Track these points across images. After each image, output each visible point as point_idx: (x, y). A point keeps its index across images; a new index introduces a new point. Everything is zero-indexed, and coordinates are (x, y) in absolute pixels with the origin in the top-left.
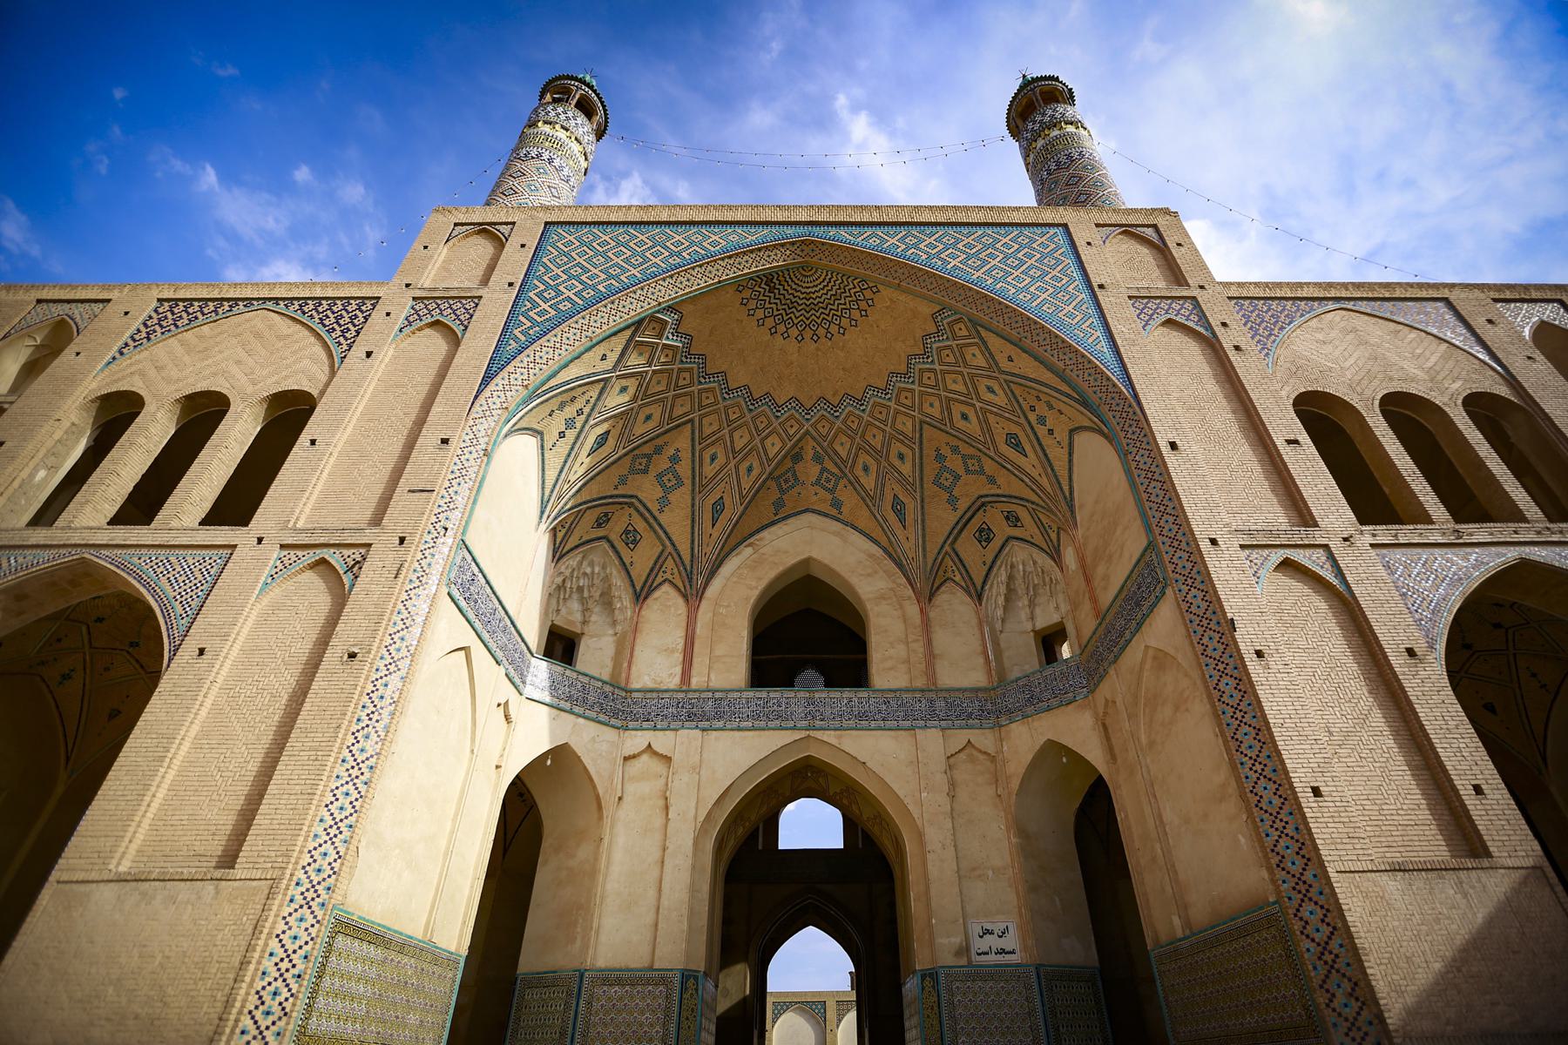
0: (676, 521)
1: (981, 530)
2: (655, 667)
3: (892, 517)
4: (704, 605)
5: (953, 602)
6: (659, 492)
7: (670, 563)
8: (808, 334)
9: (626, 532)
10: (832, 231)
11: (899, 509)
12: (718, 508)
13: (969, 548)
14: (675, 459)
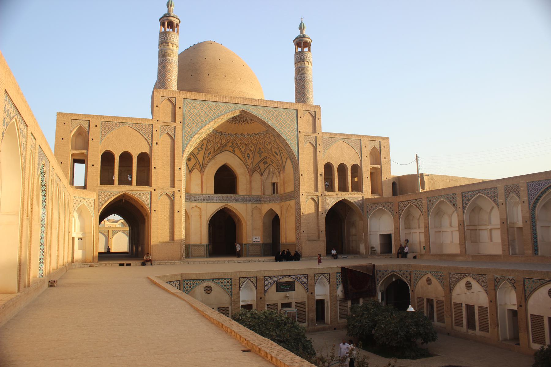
0: (200, 157)
2: (196, 189)
3: (246, 157)
4: (205, 174)
5: (257, 176)
10: (248, 106)
11: (248, 156)
12: (209, 154)
13: (262, 166)
14: (202, 145)
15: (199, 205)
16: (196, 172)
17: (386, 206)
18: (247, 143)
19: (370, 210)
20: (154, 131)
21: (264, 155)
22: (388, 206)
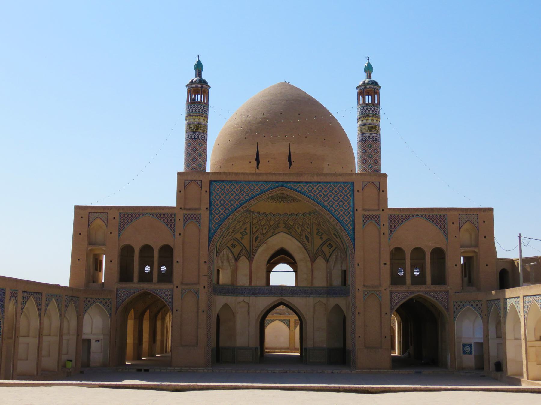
0: (246, 242)
1: (329, 245)
2: (243, 280)
3: (305, 240)
4: (254, 262)
5: (320, 261)
6: (241, 236)
7: (244, 251)
8: (282, 202)
9: (232, 245)
12: (257, 238)
13: (326, 249)
14: (245, 229)
15: (247, 299)
16: (243, 260)
17: (474, 305)
18: (301, 223)
19: (457, 309)
20: (177, 220)
21: (325, 237)
22: (477, 305)
